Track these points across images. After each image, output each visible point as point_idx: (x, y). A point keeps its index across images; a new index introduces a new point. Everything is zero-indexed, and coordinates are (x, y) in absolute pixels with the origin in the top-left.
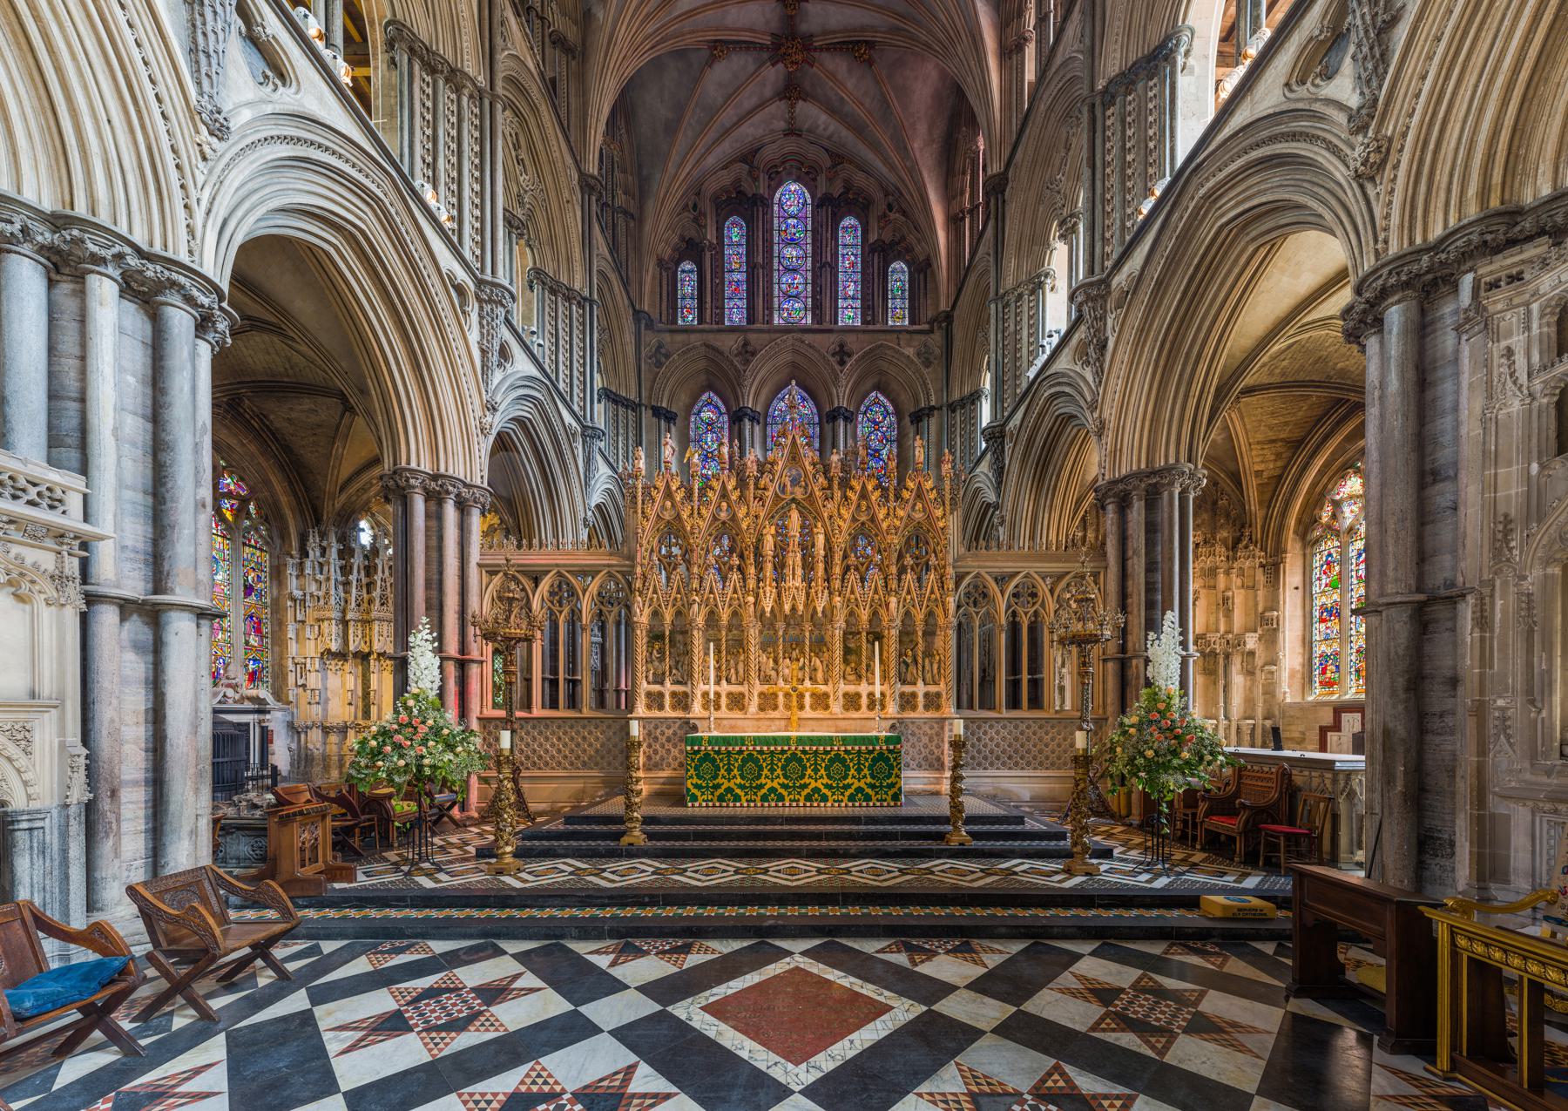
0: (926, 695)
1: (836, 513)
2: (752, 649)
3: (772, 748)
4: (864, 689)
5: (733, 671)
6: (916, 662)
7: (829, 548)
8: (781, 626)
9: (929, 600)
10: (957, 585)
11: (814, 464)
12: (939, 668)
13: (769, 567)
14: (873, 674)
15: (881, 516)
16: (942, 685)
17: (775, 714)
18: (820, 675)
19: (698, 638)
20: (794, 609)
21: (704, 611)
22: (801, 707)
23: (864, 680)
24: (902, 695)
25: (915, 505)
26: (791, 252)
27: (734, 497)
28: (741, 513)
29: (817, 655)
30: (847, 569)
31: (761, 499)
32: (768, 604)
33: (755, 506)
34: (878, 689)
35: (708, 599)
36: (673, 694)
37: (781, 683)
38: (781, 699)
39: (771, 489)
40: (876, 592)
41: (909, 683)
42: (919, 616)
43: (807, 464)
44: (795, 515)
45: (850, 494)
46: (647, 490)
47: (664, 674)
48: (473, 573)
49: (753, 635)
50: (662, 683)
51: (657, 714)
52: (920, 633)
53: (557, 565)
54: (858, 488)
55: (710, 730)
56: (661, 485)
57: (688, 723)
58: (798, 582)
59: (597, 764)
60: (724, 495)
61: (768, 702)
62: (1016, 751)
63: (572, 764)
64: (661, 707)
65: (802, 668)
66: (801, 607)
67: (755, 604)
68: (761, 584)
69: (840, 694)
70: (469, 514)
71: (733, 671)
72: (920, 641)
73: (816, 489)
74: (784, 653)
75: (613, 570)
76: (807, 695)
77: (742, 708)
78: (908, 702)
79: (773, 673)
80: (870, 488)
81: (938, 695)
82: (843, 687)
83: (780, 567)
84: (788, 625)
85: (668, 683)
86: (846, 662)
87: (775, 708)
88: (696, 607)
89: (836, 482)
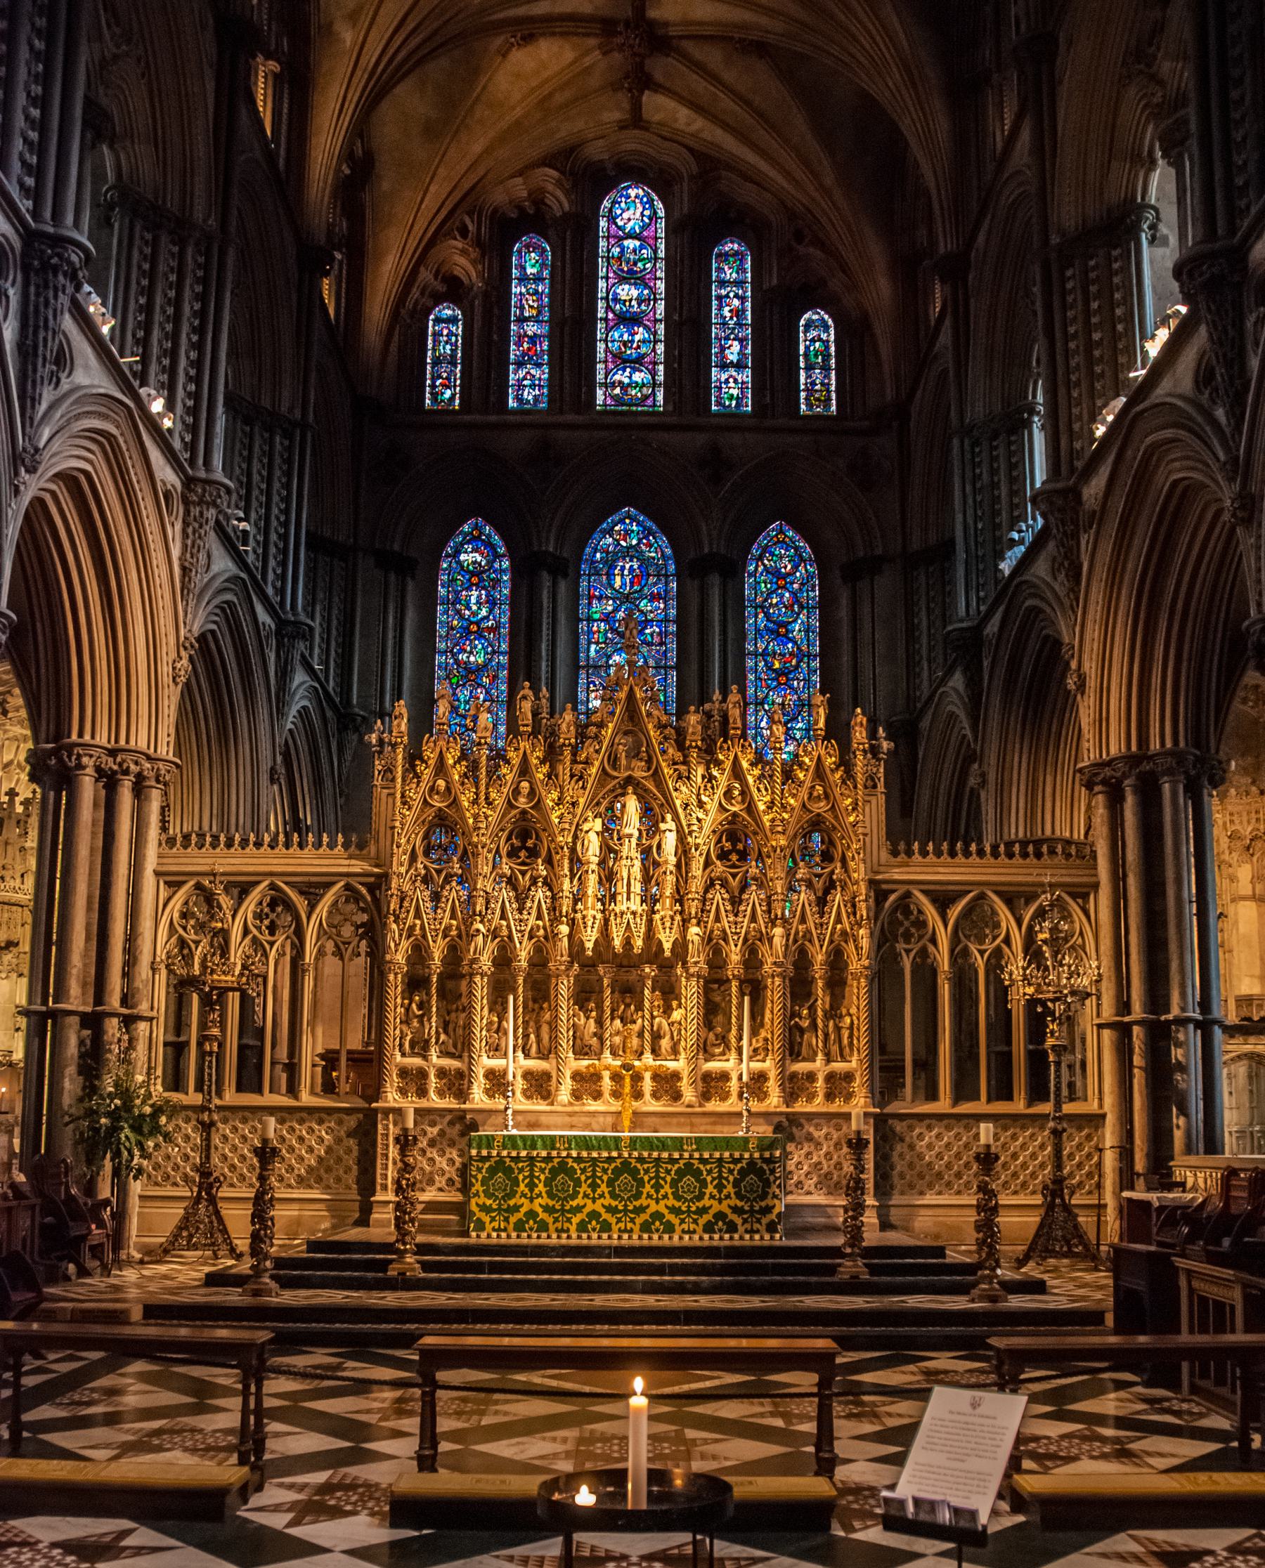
0: (830, 1078)
1: (694, 800)
3: (595, 1154)
5: (532, 1036)
6: (814, 1025)
7: (684, 851)
9: (834, 928)
11: (661, 726)
12: (851, 1036)
13: (592, 879)
15: (761, 807)
16: (854, 1064)
19: (481, 989)
20: (628, 943)
21: (492, 946)
22: (638, 1095)
24: (794, 1076)
25: (813, 787)
26: (627, 292)
28: (550, 798)
31: (581, 778)
32: (590, 938)
33: (571, 790)
37: (607, 1058)
38: (607, 1083)
39: (597, 764)
40: (753, 919)
41: (804, 1060)
42: (819, 957)
43: (650, 726)
44: (632, 805)
47: (427, 1042)
48: (149, 881)
49: (564, 988)
52: (820, 983)
53: (272, 874)
54: (728, 765)
58: (636, 905)
59: (319, 1180)
60: (525, 770)
61: (587, 1083)
66: (639, 943)
67: (570, 936)
68: (579, 906)
70: (148, 799)
71: (532, 1036)
72: (820, 992)
73: (663, 764)
74: (613, 1011)
75: (353, 882)
76: (647, 1076)
80: (745, 765)
81: (849, 1077)
83: (608, 877)
87: (597, 1096)
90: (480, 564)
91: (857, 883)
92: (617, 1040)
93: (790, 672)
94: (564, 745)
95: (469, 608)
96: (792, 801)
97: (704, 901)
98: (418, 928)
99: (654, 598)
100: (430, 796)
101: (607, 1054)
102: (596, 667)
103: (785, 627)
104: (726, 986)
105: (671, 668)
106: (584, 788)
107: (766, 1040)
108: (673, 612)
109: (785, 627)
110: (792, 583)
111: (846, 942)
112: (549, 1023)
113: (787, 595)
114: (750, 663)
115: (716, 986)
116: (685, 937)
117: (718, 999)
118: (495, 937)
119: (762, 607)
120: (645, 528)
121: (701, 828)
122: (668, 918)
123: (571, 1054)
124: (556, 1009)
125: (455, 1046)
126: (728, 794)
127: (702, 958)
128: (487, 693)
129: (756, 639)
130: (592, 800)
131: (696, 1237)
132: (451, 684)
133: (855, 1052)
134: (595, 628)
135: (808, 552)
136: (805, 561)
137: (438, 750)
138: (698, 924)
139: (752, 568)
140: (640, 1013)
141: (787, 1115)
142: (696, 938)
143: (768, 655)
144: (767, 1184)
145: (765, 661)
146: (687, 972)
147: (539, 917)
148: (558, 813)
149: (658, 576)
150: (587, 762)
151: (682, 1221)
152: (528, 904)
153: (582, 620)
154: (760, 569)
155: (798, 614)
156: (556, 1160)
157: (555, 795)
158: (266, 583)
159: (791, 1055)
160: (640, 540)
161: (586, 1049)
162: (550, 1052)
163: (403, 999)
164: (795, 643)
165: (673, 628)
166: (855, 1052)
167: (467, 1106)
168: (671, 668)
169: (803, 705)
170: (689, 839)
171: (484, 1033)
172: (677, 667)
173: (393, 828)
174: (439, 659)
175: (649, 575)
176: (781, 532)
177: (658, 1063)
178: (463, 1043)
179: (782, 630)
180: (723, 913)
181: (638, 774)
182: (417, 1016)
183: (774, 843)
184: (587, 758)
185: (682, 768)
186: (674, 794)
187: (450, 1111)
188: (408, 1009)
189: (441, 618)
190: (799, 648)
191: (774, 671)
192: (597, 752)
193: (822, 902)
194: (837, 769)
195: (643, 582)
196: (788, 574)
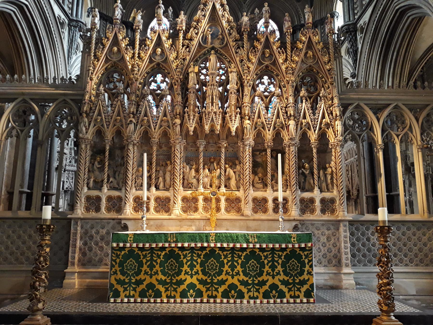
0: (323, 201)
1: (245, 57)
2: (178, 161)
4: (269, 194)
5: (161, 179)
6: (312, 173)
8: (202, 144)
9: (321, 123)
10: (343, 113)
12: (332, 178)
14: (277, 182)
15: (281, 61)
16: (335, 192)
17: (196, 216)
18: (233, 182)
20: (212, 130)
21: (140, 130)
22: (218, 209)
23: (269, 188)
24: (302, 200)
27: (167, 44)
28: (172, 56)
29: (231, 167)
31: (188, 47)
32: (192, 126)
34: (280, 195)
36: (109, 199)
37: (201, 189)
38: (201, 203)
40: (278, 116)
41: (307, 191)
42: (313, 136)
45: (256, 44)
46: (99, 41)
47: (103, 181)
50: (100, 189)
51: (93, 214)
52: (315, 151)
53: (23, 94)
54: (263, 40)
55: (142, 229)
56: (111, 36)
57: (120, 223)
62: (400, 250)
63: (17, 259)
64: (98, 209)
65: (219, 177)
67: (181, 125)
68: (186, 109)
69: (250, 199)
71: (161, 179)
76: (223, 199)
77: (168, 211)
78: (307, 207)
79: (194, 181)
80: (272, 40)
81: (333, 201)
82: (253, 193)
84: (208, 143)
85: (105, 189)
86: (255, 172)
88: (132, 126)
89: (245, 37)
91: (332, 99)
92: (206, 180)
94: (179, 29)
96: (297, 58)
100: (110, 56)
106: (189, 52)
111: (328, 129)
112: (170, 172)
115: (258, 153)
116: (242, 126)
117: (259, 160)
118: (142, 126)
122: (234, 115)
123: (181, 188)
124: (173, 163)
125: (118, 185)
130: (194, 58)
131: (258, 301)
137: (114, 32)
138: (249, 119)
141: (300, 220)
144: (303, 265)
146: (243, 144)
148: (176, 64)
150: (191, 40)
151: (249, 291)
156: (167, 250)
157: (174, 55)
158: (64, 4)
159: (299, 189)
162: (170, 187)
163: (91, 159)
167: (122, 216)
170: (244, 77)
173: (89, 70)
178: (123, 182)
182: (98, 168)
183: (288, 79)
184: (191, 37)
187: (113, 219)
188: (93, 164)
192: (197, 34)
193: (314, 108)
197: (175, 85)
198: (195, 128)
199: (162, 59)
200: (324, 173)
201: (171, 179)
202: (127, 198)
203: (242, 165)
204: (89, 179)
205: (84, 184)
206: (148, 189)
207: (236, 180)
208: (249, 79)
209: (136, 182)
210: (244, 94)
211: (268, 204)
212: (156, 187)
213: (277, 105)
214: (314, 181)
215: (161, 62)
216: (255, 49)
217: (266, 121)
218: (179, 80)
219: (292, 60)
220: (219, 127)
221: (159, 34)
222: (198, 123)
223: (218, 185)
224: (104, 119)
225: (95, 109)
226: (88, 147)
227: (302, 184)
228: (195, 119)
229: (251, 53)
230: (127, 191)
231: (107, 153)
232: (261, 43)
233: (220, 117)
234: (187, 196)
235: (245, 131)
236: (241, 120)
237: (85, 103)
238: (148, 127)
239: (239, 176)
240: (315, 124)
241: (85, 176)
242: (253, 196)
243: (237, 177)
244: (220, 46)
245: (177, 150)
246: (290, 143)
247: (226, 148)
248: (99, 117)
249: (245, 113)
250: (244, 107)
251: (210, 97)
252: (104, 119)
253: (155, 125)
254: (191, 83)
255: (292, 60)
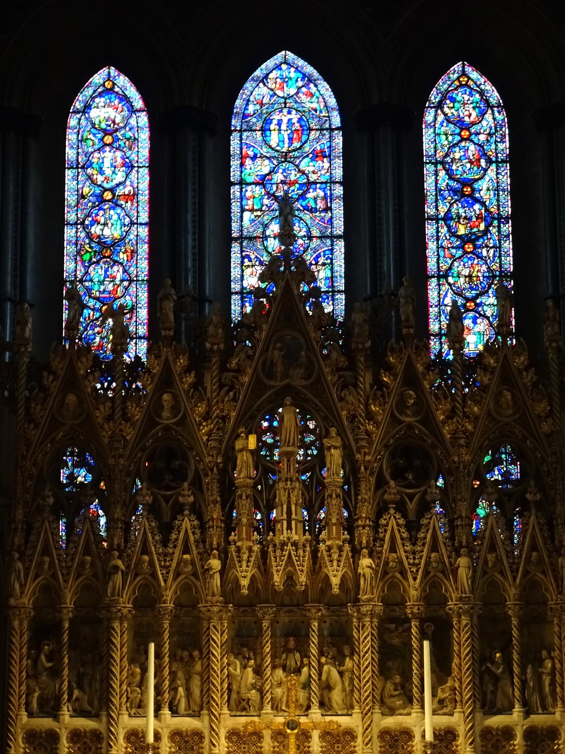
2: (217, 652)
5: (181, 690)
12: (553, 683)
16: (558, 715)
20: (290, 579)
24: (487, 733)
25: (500, 393)
30: (381, 511)
35: (139, 562)
39: (250, 371)
40: (434, 548)
52: (515, 622)
54: (400, 368)
67: (222, 572)
71: (181, 690)
73: (327, 370)
74: (273, 657)
76: (315, 735)
79: (254, 694)
80: (420, 368)
88: (118, 578)
90: (114, 122)
92: (279, 691)
93: (478, 238)
95: (101, 171)
97: (376, 527)
98: (46, 566)
99: (317, 155)
101: (268, 709)
102: (250, 239)
103: (471, 186)
104: (406, 625)
105: (339, 237)
107: (453, 689)
108: (338, 173)
109: (471, 186)
110: (477, 134)
111: (543, 572)
112: (201, 674)
113: (472, 147)
114: (430, 230)
115: (393, 626)
118: (137, 575)
119: (443, 163)
120: (304, 76)
121: (370, 443)
122: (335, 550)
123: (225, 711)
124: (207, 656)
125: (91, 703)
126: (401, 404)
127: (376, 594)
128: (125, 271)
129: (437, 201)
132: (83, 262)
133: (559, 703)
134: (248, 194)
135: (494, 96)
136: (492, 107)
138: (371, 556)
139: (429, 117)
140: (305, 661)
142: (368, 571)
143: (452, 219)
145: (449, 227)
146: (358, 611)
147: (186, 550)
149: (321, 130)
150: (239, 371)
152: (174, 536)
153: (234, 184)
154: (441, 118)
155: (486, 170)
159: (483, 707)
160: (299, 88)
161: (244, 703)
162: (202, 708)
163: (29, 649)
164: (483, 204)
165: (339, 190)
166: (559, 703)
168: (339, 237)
169: (494, 277)
171: (124, 687)
172: (346, 236)
174: (69, 233)
175: (310, 129)
176: (464, 74)
177: (328, 719)
178: (100, 699)
179: (468, 190)
180: (399, 541)
181: (298, 382)
182: (46, 669)
185: (348, 374)
186: (339, 405)
188: (36, 661)
189: (70, 184)
190: (487, 210)
191: (459, 237)
194: (527, 369)
195: (304, 138)
196: (473, 124)
197: (207, 475)
198: (253, 577)
199: (175, 417)
200: (535, 671)
201: (202, 691)
202: (113, 734)
203: (356, 658)
204: (29, 694)
205: (19, 705)
206: (157, 715)
207: (344, 690)
208: (369, 461)
209: (128, 698)
210: (360, 497)
211: (414, 743)
212: (170, 709)
213: (432, 522)
214: (513, 690)
215: (174, 424)
216: (382, 390)
217: (407, 558)
218: (215, 469)
219: (464, 412)
220: (303, 579)
221: (167, 360)
222: (259, 568)
223: (305, 704)
224: (56, 561)
225: (38, 541)
226: (25, 623)
227: (489, 696)
228: (252, 559)
229: (374, 400)
230: (113, 719)
231: (65, 635)
232: (395, 376)
233: (307, 553)
234: (238, 729)
235: (362, 582)
236: (353, 557)
237: (16, 529)
238: (149, 578)
239: (352, 680)
240: (514, 563)
241: (22, 688)
242: (381, 727)
243: (347, 683)
244: (304, 383)
245: (215, 628)
246: (460, 608)
247: (321, 621)
248: (47, 559)
249: (361, 543)
250: (358, 526)
251: (285, 507)
252: (56, 561)
253: (164, 572)
254: (242, 475)
255: (464, 412)
